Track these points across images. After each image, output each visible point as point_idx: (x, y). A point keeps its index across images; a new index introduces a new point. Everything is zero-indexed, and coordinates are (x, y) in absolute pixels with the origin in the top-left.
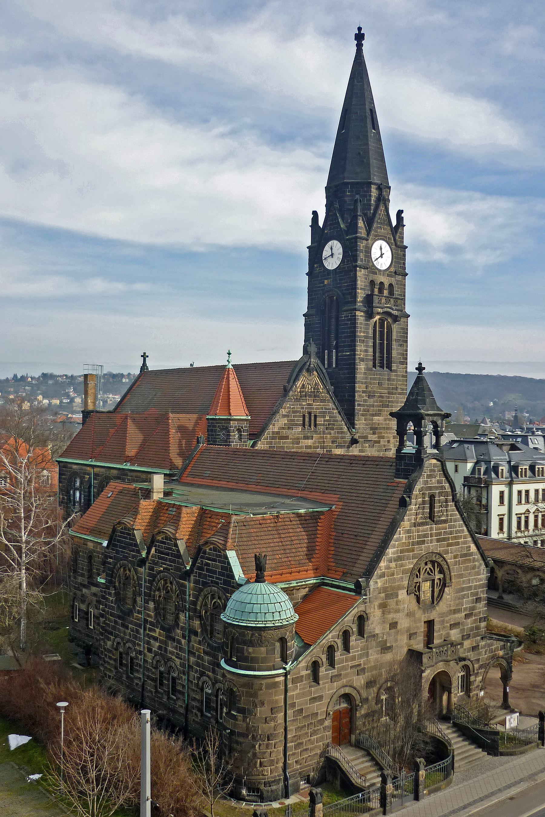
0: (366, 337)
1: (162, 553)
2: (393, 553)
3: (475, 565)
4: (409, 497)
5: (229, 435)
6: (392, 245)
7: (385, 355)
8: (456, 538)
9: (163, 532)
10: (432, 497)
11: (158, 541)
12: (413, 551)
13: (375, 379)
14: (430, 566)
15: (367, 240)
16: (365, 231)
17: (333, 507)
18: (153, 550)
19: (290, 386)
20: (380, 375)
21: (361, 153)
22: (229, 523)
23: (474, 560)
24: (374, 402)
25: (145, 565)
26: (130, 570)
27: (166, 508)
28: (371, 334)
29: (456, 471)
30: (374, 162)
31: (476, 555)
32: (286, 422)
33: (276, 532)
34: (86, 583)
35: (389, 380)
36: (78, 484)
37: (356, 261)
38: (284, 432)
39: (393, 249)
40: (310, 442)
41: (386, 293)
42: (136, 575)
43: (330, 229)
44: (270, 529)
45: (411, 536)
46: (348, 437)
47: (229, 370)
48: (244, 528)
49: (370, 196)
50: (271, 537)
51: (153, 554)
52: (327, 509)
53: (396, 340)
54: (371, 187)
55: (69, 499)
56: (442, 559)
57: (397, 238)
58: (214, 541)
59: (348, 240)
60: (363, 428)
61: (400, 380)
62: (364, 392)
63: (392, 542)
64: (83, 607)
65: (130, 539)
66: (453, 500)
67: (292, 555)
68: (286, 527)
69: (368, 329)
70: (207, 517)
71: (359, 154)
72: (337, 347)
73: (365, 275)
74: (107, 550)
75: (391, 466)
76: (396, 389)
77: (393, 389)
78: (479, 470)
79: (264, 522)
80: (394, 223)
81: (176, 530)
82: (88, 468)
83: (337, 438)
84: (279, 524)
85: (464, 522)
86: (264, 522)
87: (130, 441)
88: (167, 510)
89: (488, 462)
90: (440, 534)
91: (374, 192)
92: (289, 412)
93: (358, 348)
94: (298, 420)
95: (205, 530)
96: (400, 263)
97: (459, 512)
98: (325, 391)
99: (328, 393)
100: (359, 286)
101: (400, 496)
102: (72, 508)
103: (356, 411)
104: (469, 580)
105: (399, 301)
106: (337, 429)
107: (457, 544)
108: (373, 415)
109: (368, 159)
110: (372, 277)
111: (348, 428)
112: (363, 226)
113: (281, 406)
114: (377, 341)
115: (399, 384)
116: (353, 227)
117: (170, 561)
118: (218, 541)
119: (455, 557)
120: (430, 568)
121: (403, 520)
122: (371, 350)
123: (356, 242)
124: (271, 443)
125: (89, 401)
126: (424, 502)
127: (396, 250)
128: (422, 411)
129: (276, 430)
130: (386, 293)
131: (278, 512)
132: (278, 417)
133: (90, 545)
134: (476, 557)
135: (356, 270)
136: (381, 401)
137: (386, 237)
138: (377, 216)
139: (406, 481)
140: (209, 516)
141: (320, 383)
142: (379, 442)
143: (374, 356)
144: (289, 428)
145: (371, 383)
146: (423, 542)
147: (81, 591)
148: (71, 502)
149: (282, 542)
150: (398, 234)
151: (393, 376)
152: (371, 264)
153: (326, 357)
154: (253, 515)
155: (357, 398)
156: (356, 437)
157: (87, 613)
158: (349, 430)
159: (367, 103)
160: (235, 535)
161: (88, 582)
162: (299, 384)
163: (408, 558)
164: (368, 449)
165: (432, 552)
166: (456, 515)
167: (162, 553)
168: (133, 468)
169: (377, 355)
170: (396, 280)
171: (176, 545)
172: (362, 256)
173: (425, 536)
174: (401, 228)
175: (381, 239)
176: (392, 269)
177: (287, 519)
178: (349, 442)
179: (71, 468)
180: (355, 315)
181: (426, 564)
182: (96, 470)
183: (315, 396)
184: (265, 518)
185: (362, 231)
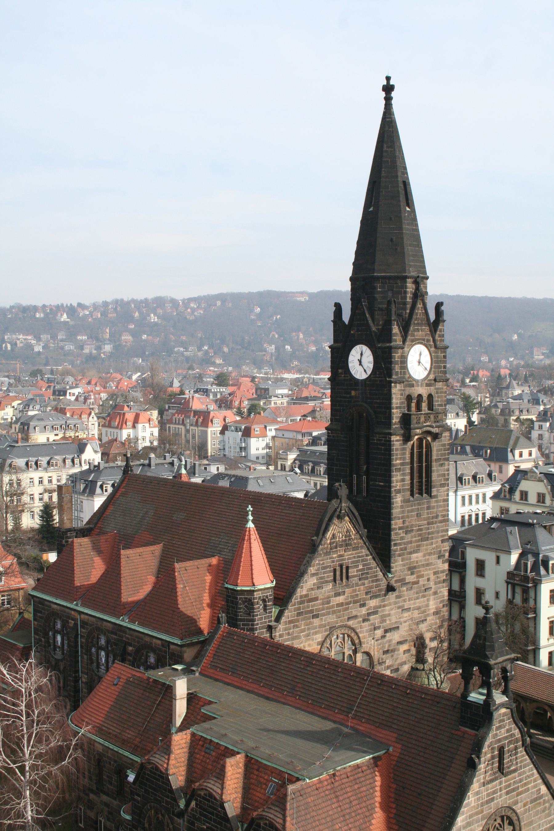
0: (402, 464)
1: (205, 810)
2: (463, 821)
3: (546, 807)
4: (479, 758)
5: (253, 609)
6: (431, 348)
7: (424, 480)
8: (526, 784)
9: (206, 790)
10: (501, 750)
11: (200, 796)
12: (482, 811)
13: (412, 511)
14: (499, 821)
15: (403, 348)
16: (400, 338)
17: (391, 749)
18: (193, 804)
19: (319, 540)
20: (419, 504)
21: (394, 238)
22: (285, 795)
23: (545, 802)
24: (412, 537)
25: (183, 817)
26: (163, 816)
27: (201, 743)
28: (408, 460)
29: (498, 562)
30: (409, 249)
31: (547, 795)
32: (315, 581)
33: (333, 795)
34: (95, 789)
35: (428, 508)
36: (59, 626)
37: (390, 376)
38: (313, 594)
39: (432, 352)
40: (341, 599)
41: (424, 405)
42: (172, 824)
43: (358, 330)
44: (327, 792)
45: (480, 797)
46: (383, 584)
47: (249, 531)
48: (301, 798)
49: (405, 292)
50: (329, 802)
51: (193, 808)
52: (384, 752)
53: (437, 460)
54: (406, 282)
55: (48, 642)
56: (511, 811)
57: (437, 337)
58: (270, 818)
59: (379, 348)
60: (400, 570)
61: (440, 506)
62: (400, 528)
63: (462, 810)
64: (92, 814)
65: (163, 782)
66: (523, 745)
67: (352, 820)
68: (343, 786)
69: (404, 454)
70: (253, 769)
71: (392, 240)
72: (367, 473)
73: (401, 390)
74: (133, 786)
75: (455, 707)
76: (437, 517)
77: (433, 518)
78: (526, 565)
79: (321, 785)
80: (432, 317)
81: (222, 789)
82: (73, 612)
83: (371, 587)
84: (336, 784)
85: (535, 765)
86: (321, 785)
87: (125, 587)
88: (203, 746)
89: (536, 555)
90: (509, 785)
91: (410, 287)
92: (318, 569)
93: (394, 479)
94: (328, 577)
95: (252, 786)
96: (440, 367)
97: (529, 756)
98: (358, 536)
99: (361, 538)
100: (394, 405)
101: (468, 756)
102: (52, 653)
103: (392, 553)
104: (539, 825)
105: (440, 416)
106: (371, 577)
107: (528, 790)
108: (411, 553)
109: (403, 248)
110: (409, 391)
111: (383, 574)
112: (398, 332)
113: (309, 564)
114: (415, 465)
115: (439, 511)
116: (386, 335)
117: (215, 821)
118: (275, 818)
119: (525, 805)
120: (499, 824)
121: (471, 782)
122: (408, 478)
123: (390, 353)
124: (299, 609)
125: (65, 518)
126: (493, 757)
127: (436, 352)
128: (492, 662)
129: (304, 592)
130: (424, 405)
131: (335, 769)
132: (306, 577)
133: (100, 748)
134: (546, 798)
135: (390, 387)
136: (420, 535)
137: (424, 340)
138: (414, 317)
139: (474, 732)
140: (256, 767)
141: (352, 528)
142: (417, 583)
143: (412, 484)
144: (318, 588)
145: (408, 517)
146: (493, 799)
147: (88, 795)
148: (50, 646)
149: (340, 806)
150: (438, 333)
151: (433, 501)
152: (407, 376)
153: (355, 482)
154: (310, 779)
155: (393, 537)
156: (393, 582)
157: (96, 822)
158: (384, 576)
159: (399, 174)
160: (292, 810)
161: (97, 788)
162: (329, 535)
163: (477, 821)
164: (405, 593)
165: (502, 807)
166: (526, 760)
167: (205, 810)
168: (133, 627)
169: (415, 481)
170: (436, 389)
171: (223, 808)
172: (397, 368)
173: (494, 792)
174: (441, 324)
175: (419, 343)
176: (432, 377)
177: (343, 776)
178: (385, 590)
179: (50, 607)
180: (390, 441)
181: (495, 820)
182: (83, 616)
183: (347, 545)
184: (322, 780)
185: (397, 340)
